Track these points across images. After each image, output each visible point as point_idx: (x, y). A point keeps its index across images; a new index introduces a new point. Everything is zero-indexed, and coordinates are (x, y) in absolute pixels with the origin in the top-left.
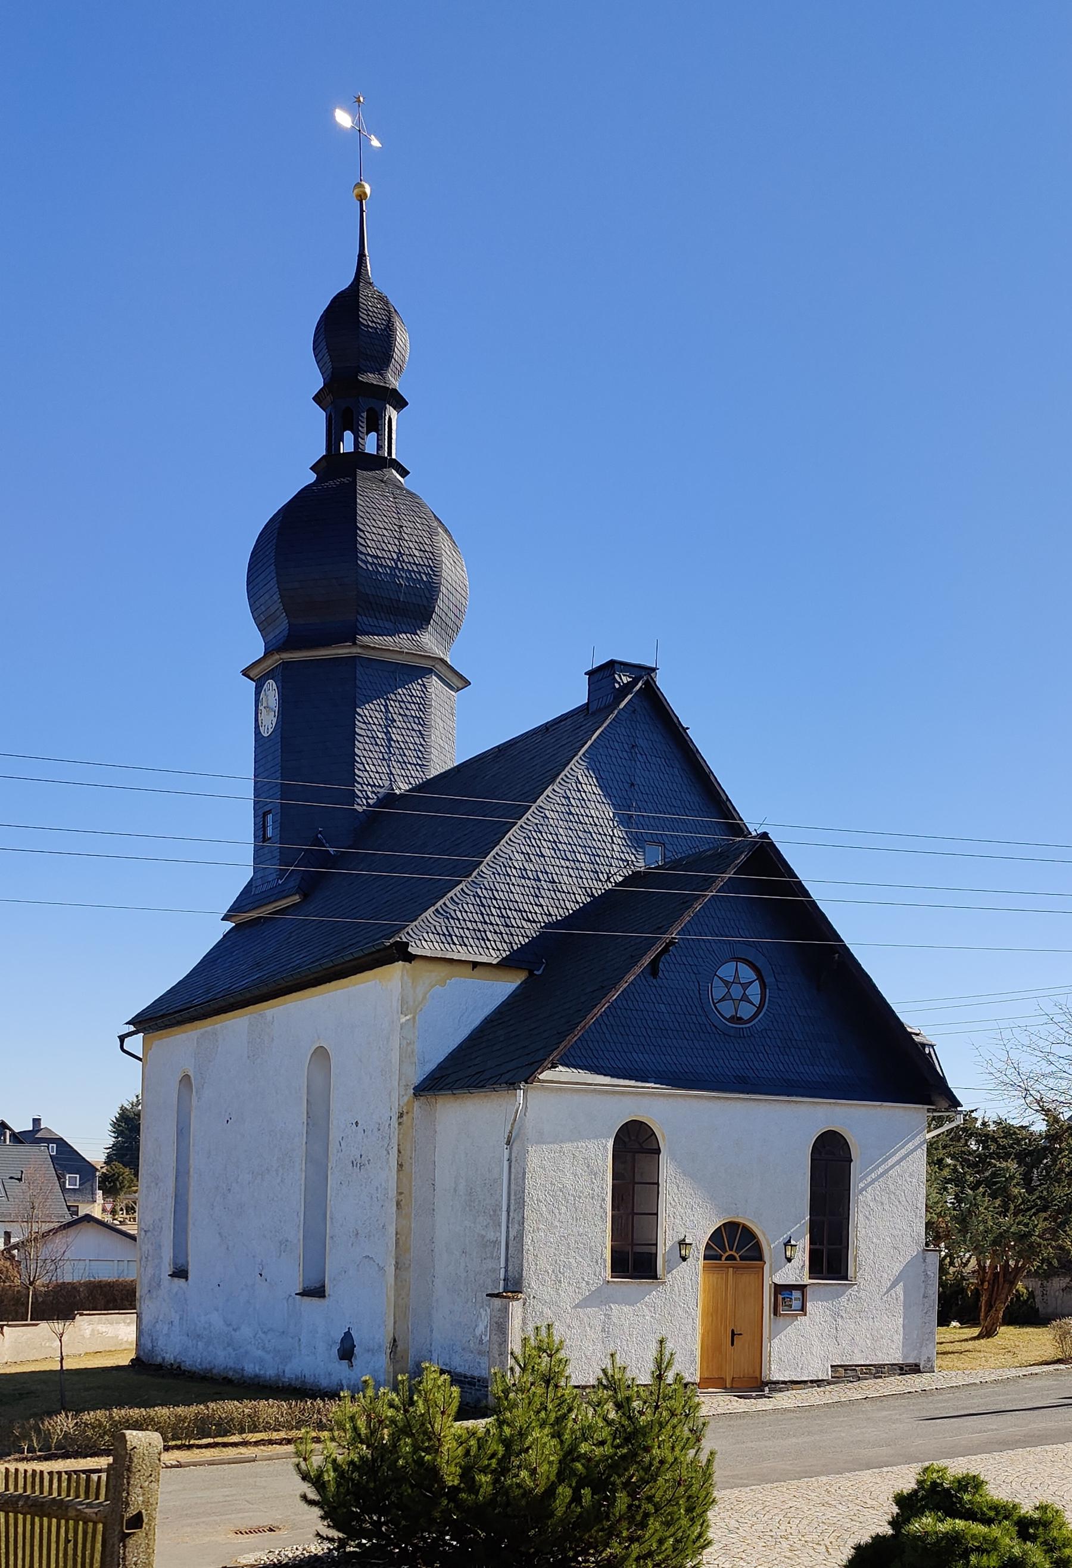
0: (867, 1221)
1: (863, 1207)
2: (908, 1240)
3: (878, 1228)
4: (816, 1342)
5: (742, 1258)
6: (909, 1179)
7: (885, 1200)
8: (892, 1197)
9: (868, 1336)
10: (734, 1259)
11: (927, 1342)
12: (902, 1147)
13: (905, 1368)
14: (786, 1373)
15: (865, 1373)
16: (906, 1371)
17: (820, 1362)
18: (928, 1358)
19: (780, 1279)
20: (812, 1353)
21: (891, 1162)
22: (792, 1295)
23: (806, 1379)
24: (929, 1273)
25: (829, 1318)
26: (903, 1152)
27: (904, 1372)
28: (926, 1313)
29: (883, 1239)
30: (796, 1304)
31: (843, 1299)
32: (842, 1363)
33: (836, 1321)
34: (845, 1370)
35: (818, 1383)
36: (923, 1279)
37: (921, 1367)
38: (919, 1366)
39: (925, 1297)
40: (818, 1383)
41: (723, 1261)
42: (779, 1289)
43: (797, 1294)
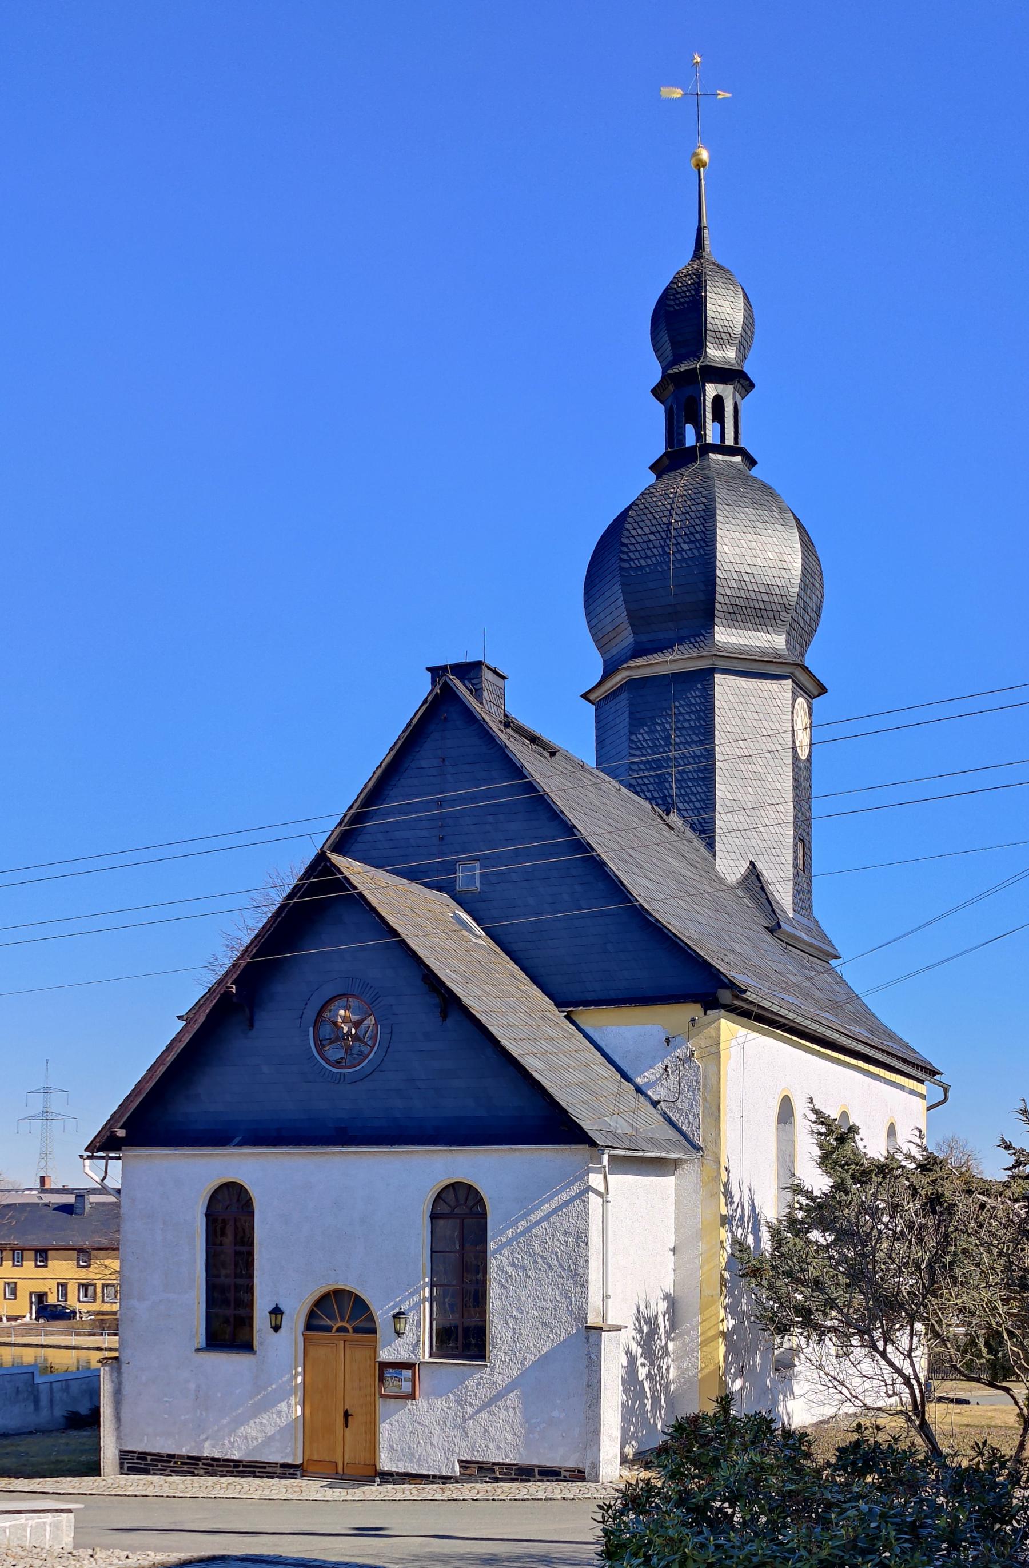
0: (503, 1290)
1: (497, 1273)
2: (565, 1316)
3: (519, 1299)
4: (437, 1431)
5: (356, 1330)
6: (562, 1238)
7: (528, 1263)
8: (539, 1260)
9: (508, 1429)
10: (348, 1332)
11: (592, 1443)
12: (551, 1197)
13: (563, 1473)
14: (401, 1464)
15: (505, 1474)
16: (565, 1477)
17: (443, 1455)
18: (592, 1463)
19: (385, 1355)
20: (432, 1444)
21: (534, 1218)
22: (401, 1374)
23: (425, 1472)
24: (593, 1356)
25: (453, 1405)
26: (554, 1204)
27: (562, 1477)
28: (589, 1407)
29: (528, 1313)
30: (406, 1386)
31: (470, 1383)
32: (474, 1459)
33: (463, 1408)
34: (479, 1467)
35: (445, 1479)
36: (586, 1362)
37: (586, 1474)
38: (584, 1473)
39: (589, 1386)
40: (445, 1479)
41: (333, 1333)
42: (385, 1365)
43: (407, 1373)
